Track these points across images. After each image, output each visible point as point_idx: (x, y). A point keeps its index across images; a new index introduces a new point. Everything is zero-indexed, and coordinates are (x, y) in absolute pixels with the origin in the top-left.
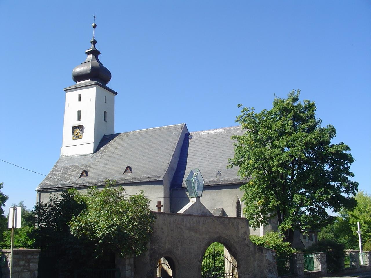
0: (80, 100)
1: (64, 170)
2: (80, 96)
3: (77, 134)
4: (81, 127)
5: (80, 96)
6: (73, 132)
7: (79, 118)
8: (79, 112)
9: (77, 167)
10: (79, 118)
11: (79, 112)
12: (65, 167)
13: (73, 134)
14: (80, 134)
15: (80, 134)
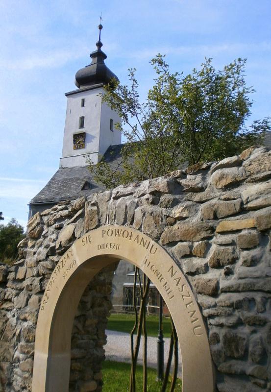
0: (83, 105)
1: (63, 183)
2: (83, 100)
3: (79, 143)
4: (83, 135)
5: (83, 100)
6: (74, 141)
7: (82, 126)
8: (82, 119)
9: (77, 179)
10: (82, 126)
11: (82, 119)
12: (64, 180)
13: (74, 144)
14: (82, 143)
15: (82, 143)
